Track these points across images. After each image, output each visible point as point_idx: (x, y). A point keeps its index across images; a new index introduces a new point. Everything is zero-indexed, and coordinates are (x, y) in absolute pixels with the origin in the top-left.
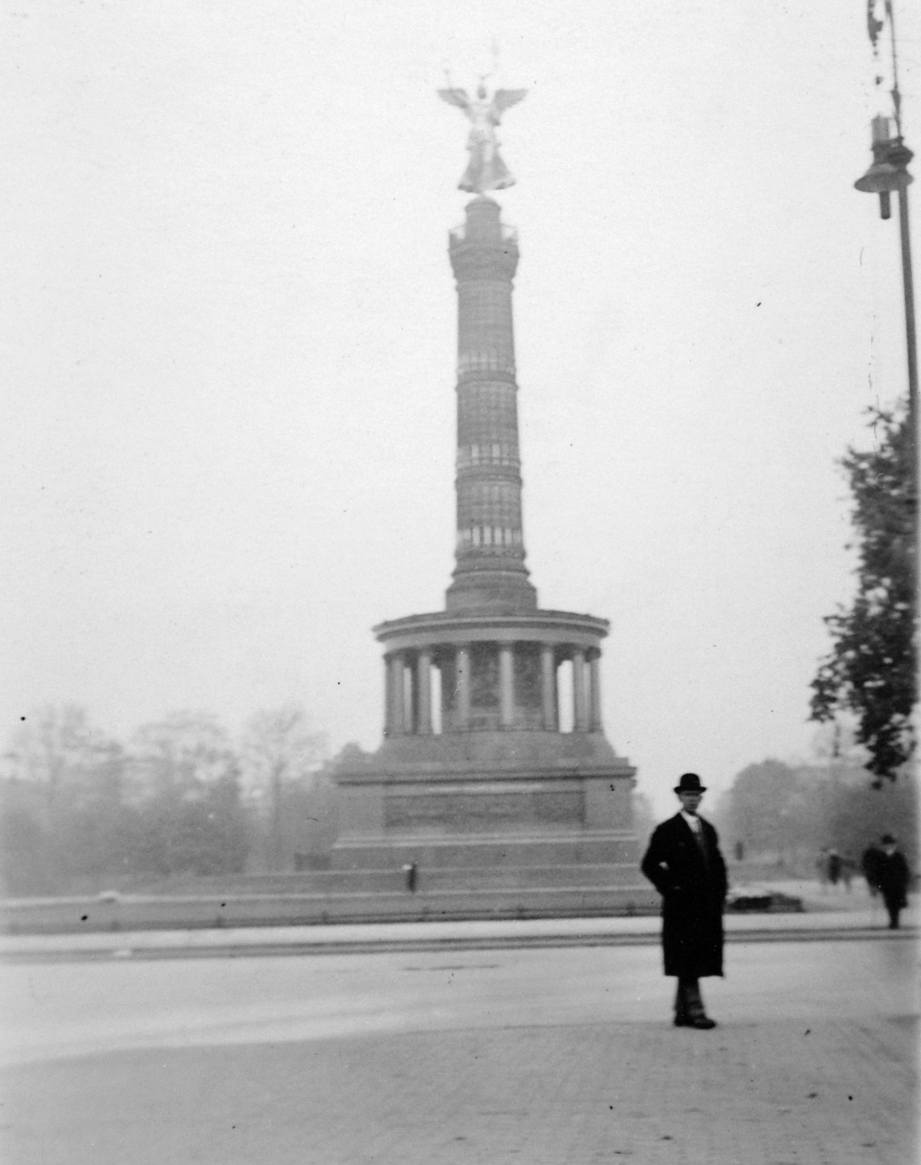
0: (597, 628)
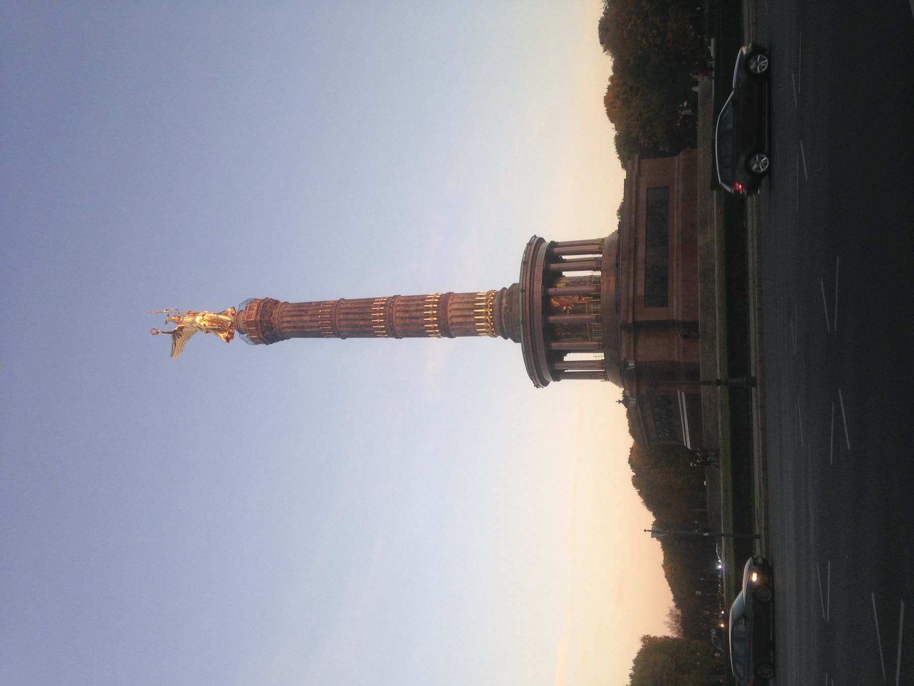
0: (536, 243)
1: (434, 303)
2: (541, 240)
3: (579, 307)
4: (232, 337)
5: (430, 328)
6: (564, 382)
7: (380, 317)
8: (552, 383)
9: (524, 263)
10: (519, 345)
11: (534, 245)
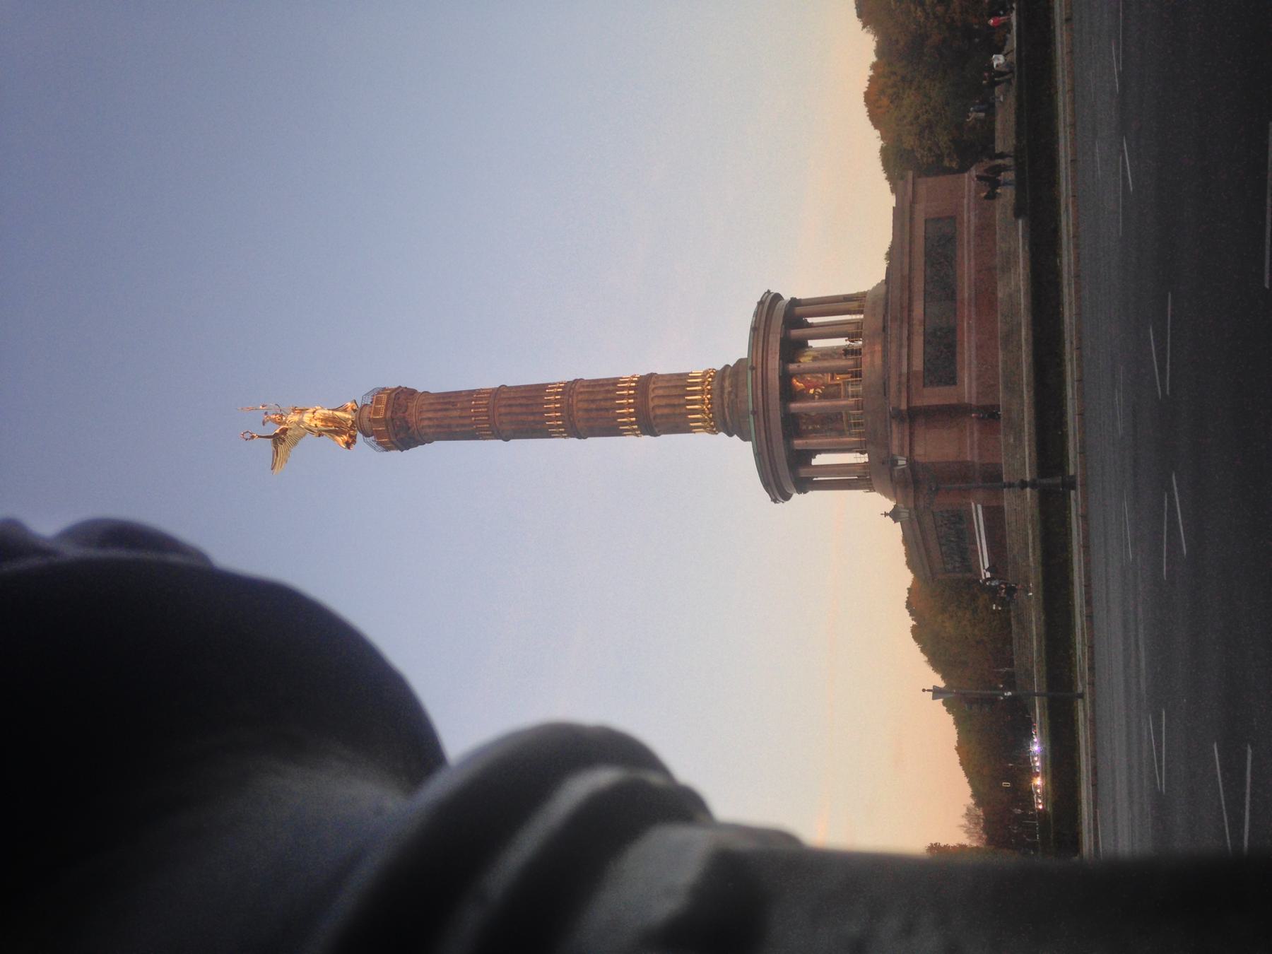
0: (770, 303)
1: (630, 388)
2: (778, 297)
3: (832, 390)
4: (354, 442)
5: (624, 424)
6: (814, 495)
7: (556, 410)
8: (796, 496)
9: (754, 329)
10: (749, 444)
11: (767, 304)
